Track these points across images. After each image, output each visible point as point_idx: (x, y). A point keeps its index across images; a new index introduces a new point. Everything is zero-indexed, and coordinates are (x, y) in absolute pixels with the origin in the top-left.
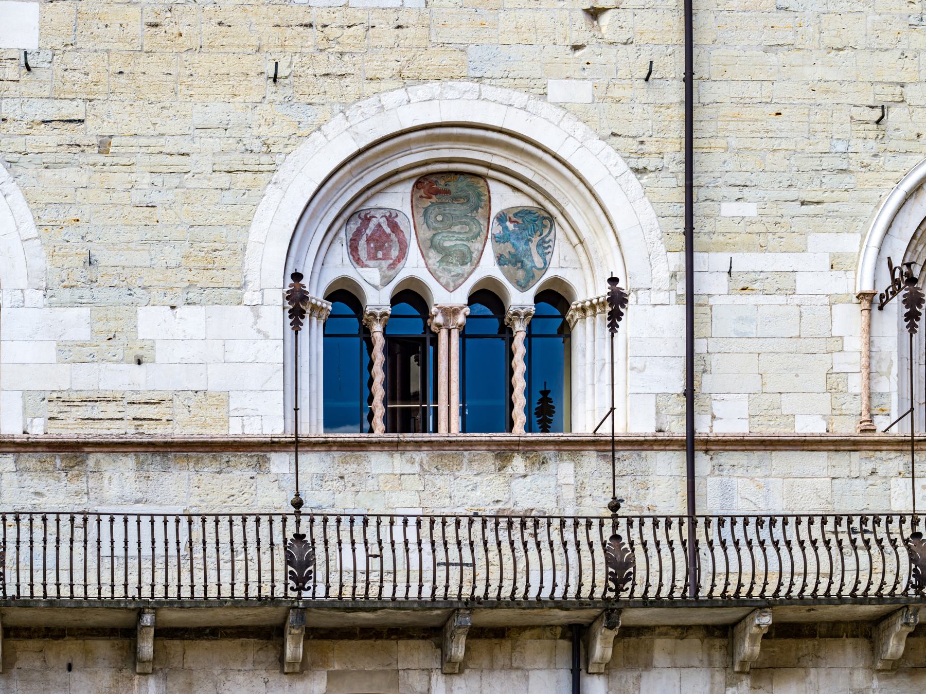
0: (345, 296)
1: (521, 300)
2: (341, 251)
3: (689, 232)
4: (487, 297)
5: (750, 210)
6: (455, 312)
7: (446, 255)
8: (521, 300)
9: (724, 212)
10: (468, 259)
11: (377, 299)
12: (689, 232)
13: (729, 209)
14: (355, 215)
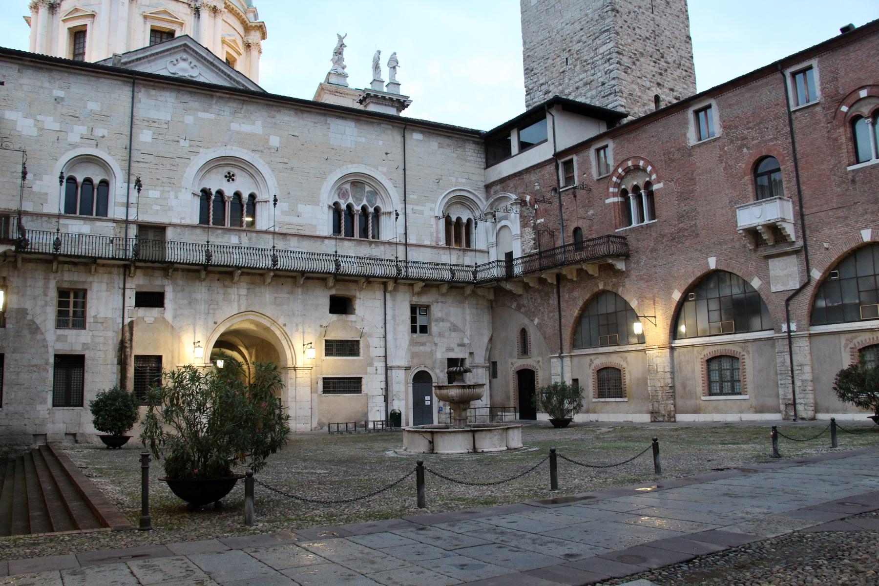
2: (336, 196)
4: (364, 208)
5: (415, 197)
6: (358, 211)
7: (357, 199)
9: (411, 197)
10: (361, 200)
11: (344, 207)
12: (405, 200)
13: (412, 196)
14: (339, 188)
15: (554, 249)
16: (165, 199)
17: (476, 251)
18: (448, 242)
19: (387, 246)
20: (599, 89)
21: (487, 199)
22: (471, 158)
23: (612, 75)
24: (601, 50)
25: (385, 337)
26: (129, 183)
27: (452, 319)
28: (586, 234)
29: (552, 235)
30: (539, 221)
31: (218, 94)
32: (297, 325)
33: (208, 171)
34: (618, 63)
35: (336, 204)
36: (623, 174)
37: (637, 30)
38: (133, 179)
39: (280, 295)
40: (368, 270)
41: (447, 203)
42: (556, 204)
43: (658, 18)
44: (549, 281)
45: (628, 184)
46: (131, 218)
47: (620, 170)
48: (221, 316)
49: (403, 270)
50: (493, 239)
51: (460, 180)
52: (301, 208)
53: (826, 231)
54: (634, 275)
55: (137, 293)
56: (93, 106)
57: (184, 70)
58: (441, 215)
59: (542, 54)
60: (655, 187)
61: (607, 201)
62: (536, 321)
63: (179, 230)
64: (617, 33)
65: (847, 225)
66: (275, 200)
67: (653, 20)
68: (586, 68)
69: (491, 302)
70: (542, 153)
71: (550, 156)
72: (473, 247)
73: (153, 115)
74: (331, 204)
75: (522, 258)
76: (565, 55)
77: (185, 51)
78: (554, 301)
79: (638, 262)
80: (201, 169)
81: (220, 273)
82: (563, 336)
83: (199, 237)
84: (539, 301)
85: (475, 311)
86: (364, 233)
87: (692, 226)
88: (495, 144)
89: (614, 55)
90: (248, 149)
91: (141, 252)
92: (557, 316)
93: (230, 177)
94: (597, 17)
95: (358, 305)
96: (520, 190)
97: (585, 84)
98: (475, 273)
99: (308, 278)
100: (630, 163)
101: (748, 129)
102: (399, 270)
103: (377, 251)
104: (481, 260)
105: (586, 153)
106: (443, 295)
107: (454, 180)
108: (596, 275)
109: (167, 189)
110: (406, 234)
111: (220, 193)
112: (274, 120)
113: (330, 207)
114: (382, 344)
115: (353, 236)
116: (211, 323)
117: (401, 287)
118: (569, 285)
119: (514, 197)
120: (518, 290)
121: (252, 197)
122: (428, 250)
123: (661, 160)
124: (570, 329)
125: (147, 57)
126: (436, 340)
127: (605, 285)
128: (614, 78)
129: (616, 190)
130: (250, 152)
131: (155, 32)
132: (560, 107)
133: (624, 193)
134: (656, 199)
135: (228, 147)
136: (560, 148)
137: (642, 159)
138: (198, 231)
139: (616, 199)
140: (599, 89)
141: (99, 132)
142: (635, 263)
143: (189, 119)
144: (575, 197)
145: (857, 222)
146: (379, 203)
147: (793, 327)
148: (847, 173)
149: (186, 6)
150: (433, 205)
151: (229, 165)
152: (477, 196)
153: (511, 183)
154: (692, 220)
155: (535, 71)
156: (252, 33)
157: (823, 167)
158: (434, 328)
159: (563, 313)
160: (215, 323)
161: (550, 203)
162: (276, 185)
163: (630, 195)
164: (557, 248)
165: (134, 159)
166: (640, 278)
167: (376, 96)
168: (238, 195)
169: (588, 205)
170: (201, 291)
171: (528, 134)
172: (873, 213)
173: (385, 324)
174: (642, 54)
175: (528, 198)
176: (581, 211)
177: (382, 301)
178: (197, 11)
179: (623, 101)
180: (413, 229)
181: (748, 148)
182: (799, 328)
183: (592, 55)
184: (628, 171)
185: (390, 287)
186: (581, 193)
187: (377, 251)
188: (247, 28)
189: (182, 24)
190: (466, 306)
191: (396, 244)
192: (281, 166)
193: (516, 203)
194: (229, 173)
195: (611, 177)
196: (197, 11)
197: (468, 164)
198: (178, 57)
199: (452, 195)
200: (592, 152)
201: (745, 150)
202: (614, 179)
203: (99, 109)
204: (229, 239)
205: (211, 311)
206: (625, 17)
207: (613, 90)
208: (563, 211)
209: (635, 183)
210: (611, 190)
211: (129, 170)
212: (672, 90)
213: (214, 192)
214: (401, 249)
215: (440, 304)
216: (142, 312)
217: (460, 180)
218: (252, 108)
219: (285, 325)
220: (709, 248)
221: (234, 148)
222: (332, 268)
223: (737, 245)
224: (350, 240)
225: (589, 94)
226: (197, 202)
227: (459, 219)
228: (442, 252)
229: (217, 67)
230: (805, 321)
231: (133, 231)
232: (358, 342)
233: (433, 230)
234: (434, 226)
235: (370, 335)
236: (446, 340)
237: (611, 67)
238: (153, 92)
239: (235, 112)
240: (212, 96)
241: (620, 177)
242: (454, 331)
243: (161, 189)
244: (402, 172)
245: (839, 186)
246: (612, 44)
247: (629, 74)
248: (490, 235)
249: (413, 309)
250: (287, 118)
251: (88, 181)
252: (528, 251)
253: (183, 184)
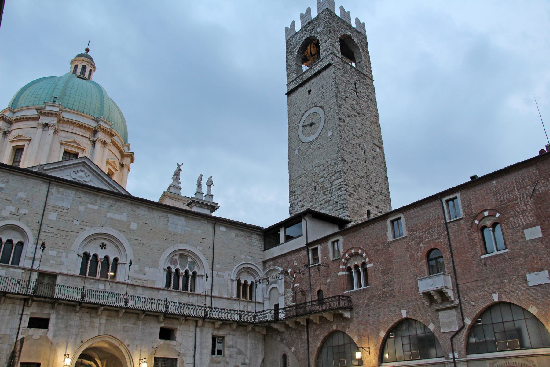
0: (169, 268)
1: (191, 273)
2: (170, 263)
3: (213, 268)
4: (186, 272)
5: (219, 267)
6: (182, 273)
7: (182, 266)
8: (191, 273)
9: (217, 266)
11: (173, 270)
12: (213, 268)
13: (217, 266)
14: (172, 258)
15: (305, 303)
16: (59, 257)
17: (256, 302)
18: (238, 296)
19: (199, 297)
20: (334, 205)
21: (264, 269)
22: (255, 244)
23: (342, 197)
24: (335, 183)
25: (194, 357)
26: (37, 245)
27: (239, 347)
28: (325, 294)
29: (304, 294)
30: (296, 285)
31: (101, 194)
32: (137, 346)
33: (90, 241)
34: (346, 190)
35: (169, 268)
36: (349, 257)
37: (357, 172)
38: (40, 242)
39: (128, 325)
40: (186, 312)
41: (239, 271)
42: (307, 275)
43: (368, 166)
44: (302, 323)
45: (351, 264)
46: (35, 268)
47: (347, 255)
48: (86, 338)
49: (209, 313)
50: (267, 295)
51: (248, 257)
52: (146, 269)
53: (472, 294)
54: (355, 320)
55: (31, 318)
56: (21, 195)
57: (81, 177)
58: (235, 279)
59: (300, 183)
60: (368, 266)
61: (339, 274)
62: (293, 349)
63: (65, 278)
64: (345, 173)
65: (484, 291)
66: (131, 263)
67: (366, 166)
68: (326, 193)
69: (264, 335)
70: (300, 243)
71: (304, 245)
72: (254, 299)
73: (59, 203)
74: (166, 268)
75: (285, 308)
76: (315, 184)
77: (83, 166)
78: (304, 337)
79: (358, 313)
80: (85, 240)
81: (89, 308)
82: (310, 360)
83: (79, 283)
84: (295, 336)
85: (253, 342)
86: (185, 287)
87: (391, 291)
88: (270, 236)
89: (343, 186)
90: (117, 230)
91: (38, 291)
92: (306, 346)
93: (103, 246)
94: (333, 163)
95: (178, 334)
96: (285, 265)
97: (326, 202)
98: (254, 317)
99: (146, 315)
100: (353, 251)
101: (423, 232)
102: (206, 313)
103: (193, 300)
104: (259, 309)
105: (326, 244)
106: (234, 330)
107: (244, 257)
108: (332, 320)
109: (61, 251)
110: (212, 290)
111: (95, 256)
112: (135, 213)
113: (165, 270)
114: (192, 362)
115: (178, 289)
116: (79, 341)
117: (207, 324)
118: (314, 327)
119: (281, 269)
120: (282, 329)
121: (116, 260)
122: (225, 301)
123: (372, 250)
124: (315, 355)
125: (59, 167)
126: (228, 360)
127: (337, 327)
128: (343, 200)
129: (344, 267)
130: (117, 232)
131: (66, 152)
132: (311, 215)
133: (349, 269)
134: (369, 273)
135: (104, 227)
136: (310, 240)
137: (360, 248)
138: (78, 280)
139: (344, 273)
140: (334, 205)
141: (22, 211)
142: (356, 313)
143: (81, 208)
144: (319, 271)
145: (489, 289)
146: (196, 269)
147: (456, 355)
148: (481, 259)
149: (88, 139)
150: (230, 272)
151: (103, 239)
152: (257, 268)
153: (280, 261)
154: (391, 287)
155: (296, 193)
156: (126, 158)
157: (467, 255)
158: (227, 352)
159: (310, 345)
160: (82, 342)
161: (303, 274)
162: (132, 254)
163: (353, 270)
164: (307, 303)
165: (42, 230)
166: (359, 323)
167: (198, 202)
168: (107, 258)
169: (327, 276)
170: (75, 319)
171: (290, 231)
172: (498, 283)
173: (195, 348)
174: (359, 186)
175: (290, 270)
176: (322, 280)
177: (194, 332)
178: (94, 143)
179: (348, 213)
180: (217, 288)
181: (423, 244)
182: (460, 356)
183: (330, 185)
184: (351, 255)
185: (200, 323)
186: (322, 268)
187: (193, 300)
188: (123, 156)
189: (83, 150)
190: (248, 338)
191: (205, 296)
192: (136, 242)
193: (282, 273)
194: (103, 244)
195: (341, 259)
196: (94, 143)
197: (253, 247)
198: (79, 169)
199: (242, 266)
200: (329, 243)
201: (421, 245)
202: (343, 260)
203: (25, 197)
204: (98, 286)
205: (80, 334)
206: (349, 164)
207: (342, 206)
208: (311, 279)
209: (356, 263)
210: (341, 267)
211: (38, 236)
212: (377, 207)
213: (91, 255)
214: (208, 299)
215: (231, 336)
216: (32, 331)
217: (248, 257)
218: (121, 204)
219: (128, 345)
220: (402, 304)
221: (108, 228)
222: (163, 309)
223: (419, 303)
224: (176, 292)
225: (328, 208)
226: (80, 260)
227: (246, 282)
228: (234, 302)
229: (102, 177)
230: (463, 352)
231: (35, 276)
232: (176, 359)
233: (229, 288)
234: (230, 286)
235: (184, 355)
236: (234, 360)
237: (341, 193)
238: (61, 189)
239: (111, 206)
240: (98, 195)
241: (347, 259)
242: (240, 354)
243: (58, 250)
244: (212, 250)
245: (477, 267)
246: (342, 180)
247: (352, 197)
248: (265, 294)
249: (214, 339)
250: (143, 212)
251: (10, 241)
252: (288, 304)
253: (72, 248)
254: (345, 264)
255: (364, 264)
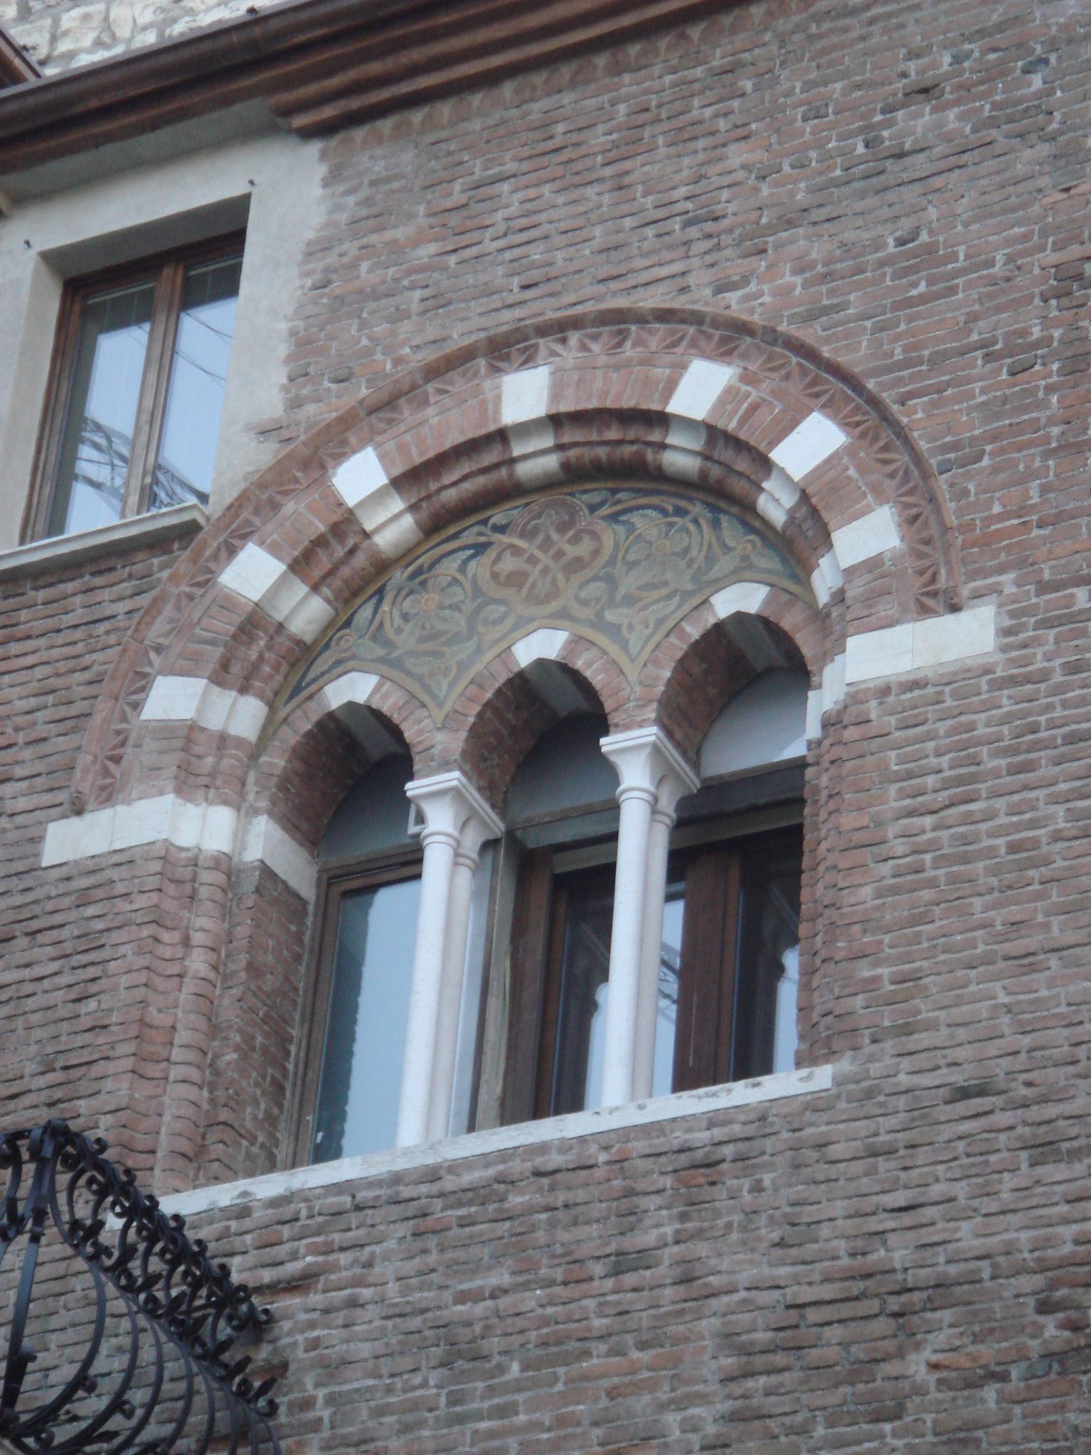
36: (392, 525)
45: (425, 683)
47: (360, 477)
61: (69, 841)
100: (524, 395)
129: (243, 715)
133: (348, 781)
137: (728, 337)
184: (467, 495)
202: (253, 573)
209: (538, 646)
210: (173, 698)
241: (342, 566)
254: (261, 655)
255: (743, 669)
